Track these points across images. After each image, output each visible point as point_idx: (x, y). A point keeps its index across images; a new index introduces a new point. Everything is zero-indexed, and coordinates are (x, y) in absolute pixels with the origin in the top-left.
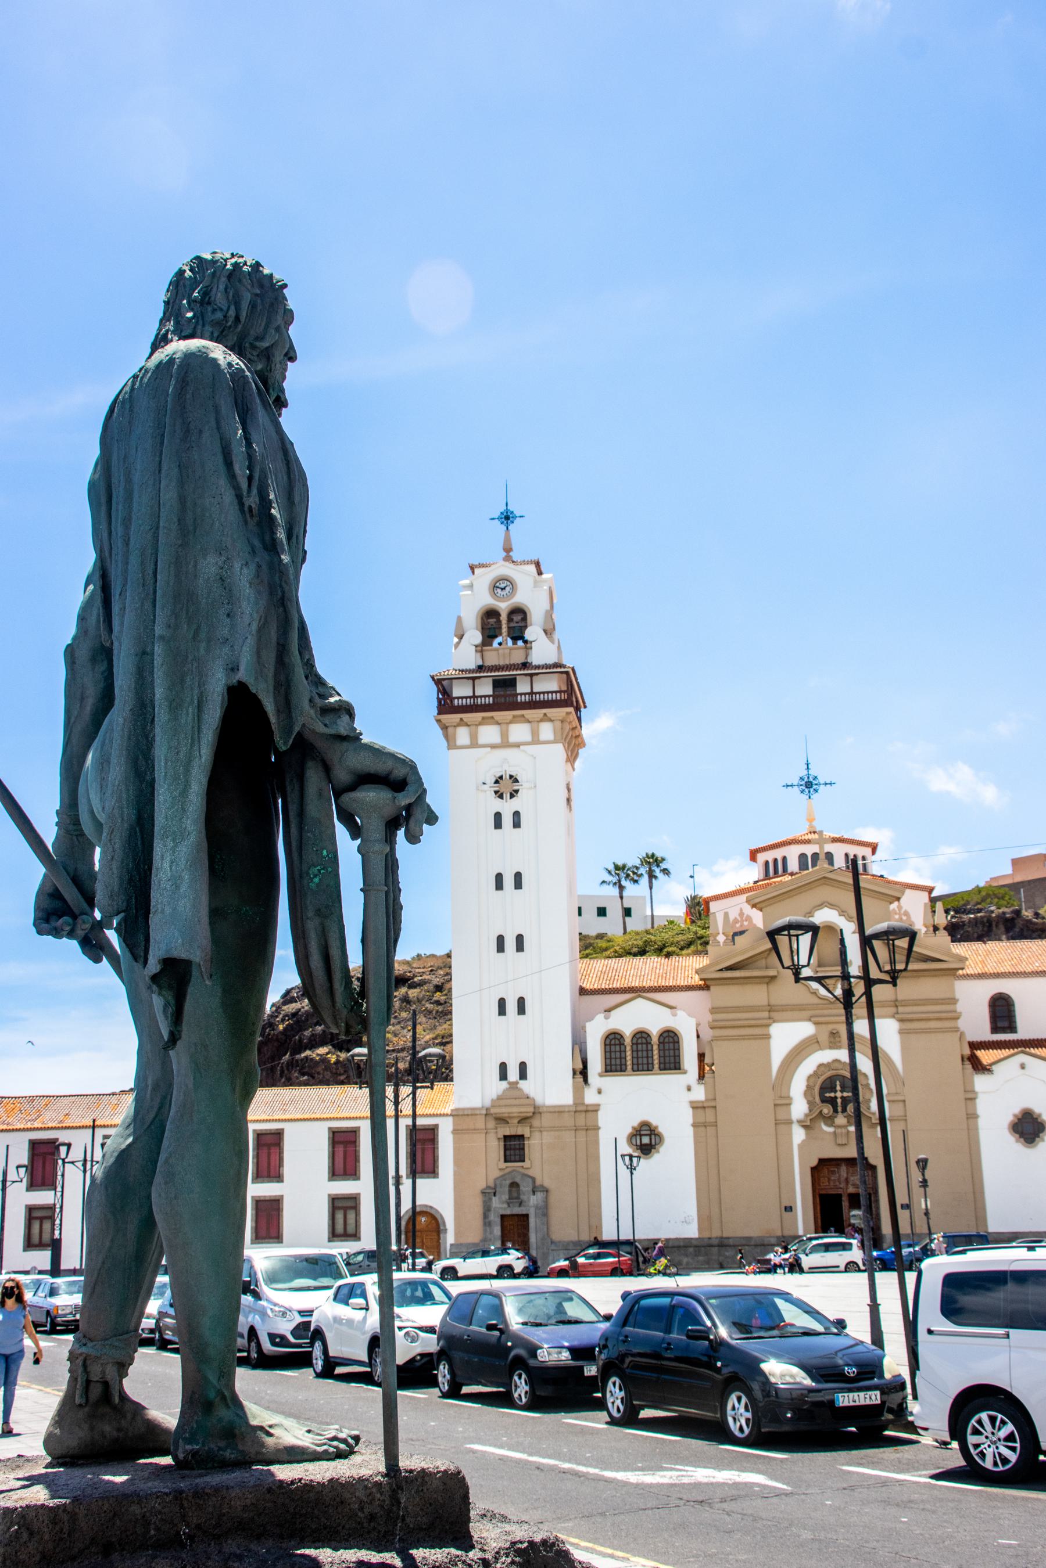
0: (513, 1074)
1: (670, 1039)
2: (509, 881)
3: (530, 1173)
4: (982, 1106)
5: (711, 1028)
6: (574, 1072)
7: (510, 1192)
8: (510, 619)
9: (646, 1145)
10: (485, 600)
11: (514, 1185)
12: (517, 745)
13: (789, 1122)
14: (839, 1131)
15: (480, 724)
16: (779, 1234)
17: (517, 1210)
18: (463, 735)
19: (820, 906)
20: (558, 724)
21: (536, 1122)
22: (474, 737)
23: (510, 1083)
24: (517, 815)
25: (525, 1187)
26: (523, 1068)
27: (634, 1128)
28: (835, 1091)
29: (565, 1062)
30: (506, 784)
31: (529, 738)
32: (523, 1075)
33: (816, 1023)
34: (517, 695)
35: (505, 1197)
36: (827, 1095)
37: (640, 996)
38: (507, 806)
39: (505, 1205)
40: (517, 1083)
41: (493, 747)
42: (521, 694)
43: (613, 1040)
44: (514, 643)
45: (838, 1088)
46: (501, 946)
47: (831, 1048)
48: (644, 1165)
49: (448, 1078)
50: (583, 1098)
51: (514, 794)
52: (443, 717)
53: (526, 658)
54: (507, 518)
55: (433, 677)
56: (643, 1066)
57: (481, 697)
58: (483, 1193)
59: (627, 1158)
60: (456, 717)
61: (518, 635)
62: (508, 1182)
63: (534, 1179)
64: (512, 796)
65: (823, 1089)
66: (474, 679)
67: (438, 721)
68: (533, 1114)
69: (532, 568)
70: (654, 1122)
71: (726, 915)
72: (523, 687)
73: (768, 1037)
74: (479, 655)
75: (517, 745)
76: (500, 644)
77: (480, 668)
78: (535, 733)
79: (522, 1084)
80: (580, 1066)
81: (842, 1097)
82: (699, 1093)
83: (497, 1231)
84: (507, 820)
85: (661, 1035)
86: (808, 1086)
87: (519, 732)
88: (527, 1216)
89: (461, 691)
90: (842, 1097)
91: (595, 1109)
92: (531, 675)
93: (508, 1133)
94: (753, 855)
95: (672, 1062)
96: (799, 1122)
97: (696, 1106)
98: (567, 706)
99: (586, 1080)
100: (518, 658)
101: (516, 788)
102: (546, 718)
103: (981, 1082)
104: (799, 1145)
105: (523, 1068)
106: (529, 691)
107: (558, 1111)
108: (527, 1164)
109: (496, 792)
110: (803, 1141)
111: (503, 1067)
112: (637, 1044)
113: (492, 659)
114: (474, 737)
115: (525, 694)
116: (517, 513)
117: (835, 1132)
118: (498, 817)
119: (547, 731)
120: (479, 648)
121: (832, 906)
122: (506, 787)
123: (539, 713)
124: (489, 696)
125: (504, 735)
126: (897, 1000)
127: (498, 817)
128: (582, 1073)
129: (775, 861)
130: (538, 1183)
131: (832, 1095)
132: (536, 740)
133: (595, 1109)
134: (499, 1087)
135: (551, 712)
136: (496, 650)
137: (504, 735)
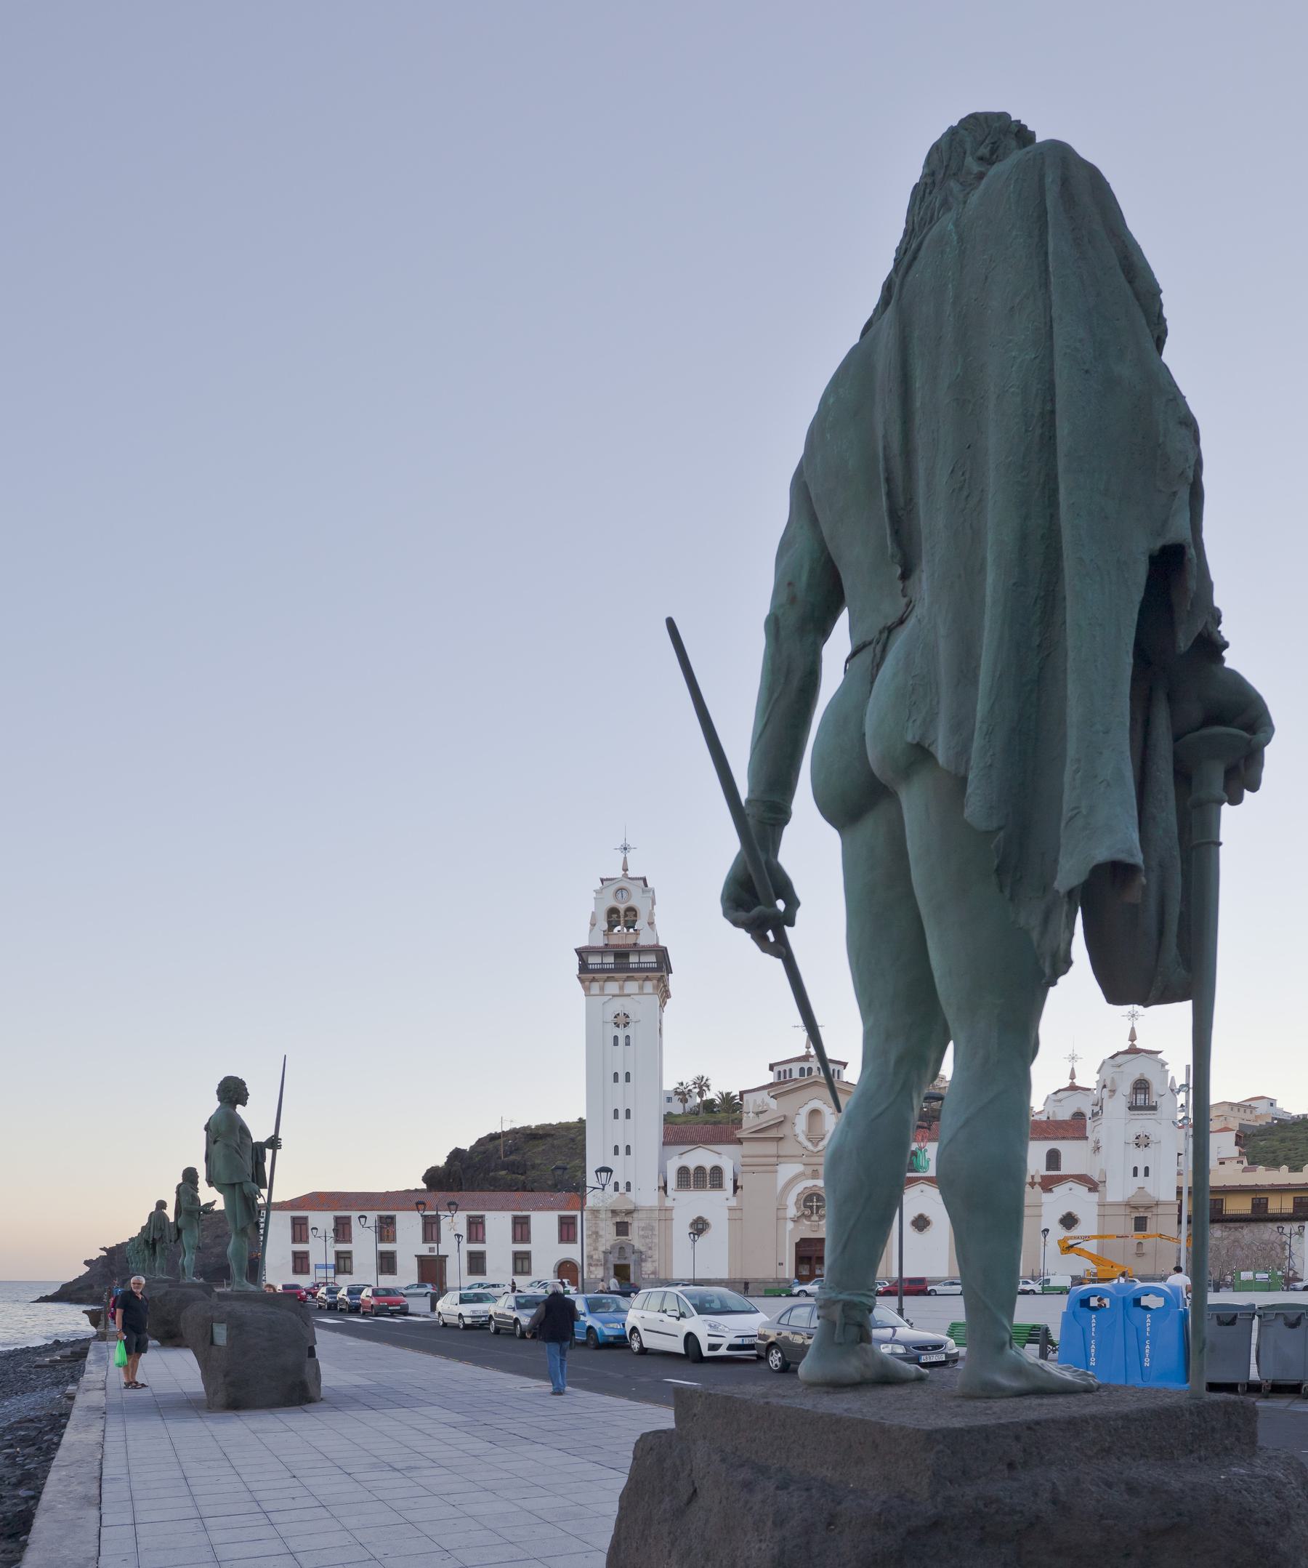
1: (717, 1171)
2: (622, 1077)
3: (632, 1242)
5: (742, 1166)
6: (659, 1187)
7: (619, 1252)
8: (626, 915)
10: (613, 903)
11: (622, 1248)
12: (629, 995)
14: (813, 1223)
15: (605, 981)
16: (775, 1277)
20: (655, 982)
21: (635, 1215)
22: (602, 989)
23: (621, 1194)
24: (628, 1037)
25: (628, 1251)
27: (694, 1220)
28: (812, 1202)
29: (655, 1183)
32: (628, 1189)
33: (804, 1164)
34: (630, 963)
35: (617, 1255)
37: (700, 1147)
38: (621, 1033)
39: (616, 1259)
40: (625, 1194)
41: (614, 996)
42: (632, 963)
43: (683, 1171)
44: (628, 931)
45: (815, 1200)
46: (616, 1116)
47: (812, 1179)
48: (701, 1240)
50: (664, 1203)
51: (626, 1024)
52: (583, 976)
53: (636, 940)
54: (625, 849)
59: (692, 1235)
60: (590, 976)
61: (630, 925)
65: (805, 1201)
69: (641, 883)
70: (706, 1217)
71: (755, 1101)
75: (629, 995)
76: (619, 931)
77: (606, 945)
78: (641, 988)
81: (817, 1206)
82: (733, 1202)
84: (621, 1041)
85: (712, 1169)
86: (797, 1200)
87: (632, 987)
89: (594, 960)
91: (669, 1210)
94: (771, 1067)
99: (666, 1192)
100: (630, 941)
102: (647, 979)
104: (790, 1231)
106: (638, 961)
107: (651, 1210)
108: (630, 1237)
113: (614, 941)
114: (602, 989)
116: (632, 846)
117: (811, 1225)
118: (616, 1038)
119: (649, 987)
122: (621, 1020)
125: (621, 988)
127: (616, 1038)
129: (785, 1071)
132: (641, 991)
133: (669, 1210)
136: (616, 934)
137: (621, 988)
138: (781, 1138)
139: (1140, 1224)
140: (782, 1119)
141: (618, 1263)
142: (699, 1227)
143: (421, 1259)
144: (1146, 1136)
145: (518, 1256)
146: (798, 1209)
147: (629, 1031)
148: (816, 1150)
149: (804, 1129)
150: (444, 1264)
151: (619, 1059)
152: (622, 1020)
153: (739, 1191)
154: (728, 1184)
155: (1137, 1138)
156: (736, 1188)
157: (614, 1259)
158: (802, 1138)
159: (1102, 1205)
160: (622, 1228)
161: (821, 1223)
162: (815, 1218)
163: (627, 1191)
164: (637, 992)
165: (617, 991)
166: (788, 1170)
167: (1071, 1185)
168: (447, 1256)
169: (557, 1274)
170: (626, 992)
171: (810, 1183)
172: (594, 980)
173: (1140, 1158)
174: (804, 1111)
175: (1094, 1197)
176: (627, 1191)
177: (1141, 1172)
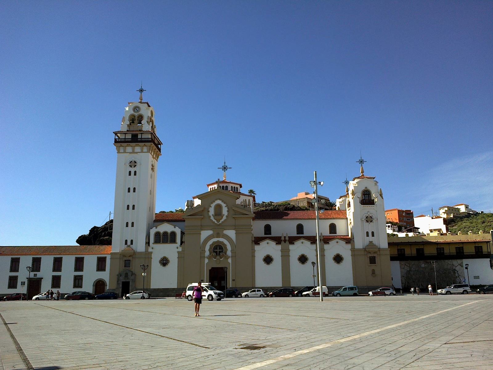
0: (129, 243)
1: (173, 234)
4: (257, 254)
6: (146, 243)
9: (165, 263)
11: (127, 274)
12: (137, 153)
17: (127, 280)
18: (122, 150)
19: (216, 200)
20: (149, 147)
24: (135, 172)
25: (129, 274)
26: (132, 241)
30: (133, 163)
33: (213, 231)
38: (133, 170)
43: (157, 234)
45: (218, 249)
47: (217, 238)
49: (111, 244)
55: (114, 132)
56: (165, 241)
57: (127, 139)
58: (117, 275)
62: (125, 272)
63: (132, 272)
64: (134, 167)
66: (125, 134)
67: (114, 145)
68: (134, 254)
72: (139, 136)
73: (200, 234)
74: (128, 127)
75: (137, 153)
79: (131, 246)
80: (148, 241)
83: (121, 286)
84: (133, 173)
87: (138, 149)
88: (129, 282)
89: (122, 136)
90: (219, 251)
92: (142, 133)
93: (126, 259)
95: (173, 241)
97: (178, 252)
98: (151, 142)
99: (149, 245)
101: (136, 164)
102: (145, 145)
103: (257, 247)
105: (132, 241)
108: (131, 268)
109: (130, 165)
110: (208, 263)
111: (126, 241)
112: (164, 235)
113: (132, 129)
115: (140, 138)
118: (130, 172)
119: (145, 149)
120: (128, 126)
121: (220, 199)
122: (133, 164)
123: (143, 144)
124: (130, 139)
125: (133, 150)
126: (235, 225)
127: (130, 172)
128: (148, 243)
130: (133, 273)
131: (216, 250)
132: (142, 152)
134: (124, 247)
135: (146, 144)
137: (133, 150)
138: (203, 218)
139: (373, 260)
140: (203, 209)
141: (124, 281)
142: (164, 262)
143: (30, 280)
144: (370, 217)
145: (77, 278)
147: (135, 169)
149: (213, 214)
150: (40, 282)
151: (132, 182)
152: (133, 164)
155: (366, 218)
156: (182, 243)
157: (122, 279)
158: (212, 218)
159: (353, 250)
160: (127, 263)
161: (221, 259)
162: (218, 257)
163: (131, 244)
164: (140, 151)
165: (131, 151)
166: (205, 234)
167: (337, 240)
168: (42, 278)
169: (94, 287)
170: (135, 151)
171: (215, 240)
172: (121, 146)
173: (370, 227)
174: (213, 205)
175: (349, 246)
176: (131, 244)
177: (370, 234)
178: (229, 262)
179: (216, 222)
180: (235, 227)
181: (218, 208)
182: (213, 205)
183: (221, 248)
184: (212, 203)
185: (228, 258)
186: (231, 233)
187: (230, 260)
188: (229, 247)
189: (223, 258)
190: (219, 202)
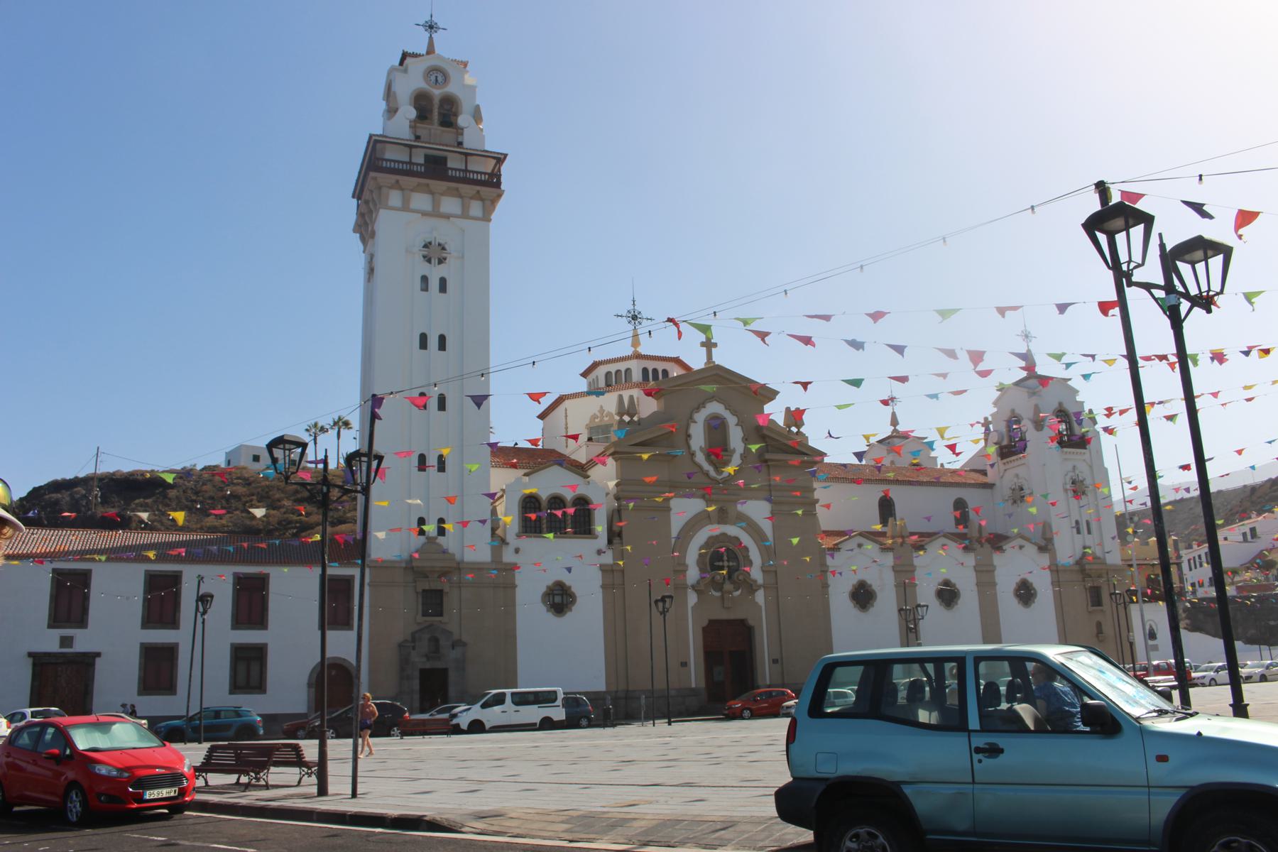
13: (685, 587)
19: (712, 398)
31: (458, 210)
36: (717, 564)
38: (435, 273)
47: (719, 523)
51: (441, 261)
84: (434, 284)
89: (392, 154)
96: (693, 587)
104: (692, 607)
109: (424, 257)
118: (425, 279)
121: (720, 401)
127: (425, 279)
131: (721, 564)
146: (702, 570)
148: (720, 477)
149: (703, 446)
152: (434, 253)
153: (616, 540)
154: (600, 528)
158: (700, 458)
178: (757, 603)
179: (712, 473)
180: (769, 494)
181: (716, 428)
182: (701, 417)
183: (732, 555)
184: (698, 409)
185: (756, 590)
186: (758, 510)
187: (760, 597)
188: (755, 555)
189: (740, 591)
190: (715, 408)
